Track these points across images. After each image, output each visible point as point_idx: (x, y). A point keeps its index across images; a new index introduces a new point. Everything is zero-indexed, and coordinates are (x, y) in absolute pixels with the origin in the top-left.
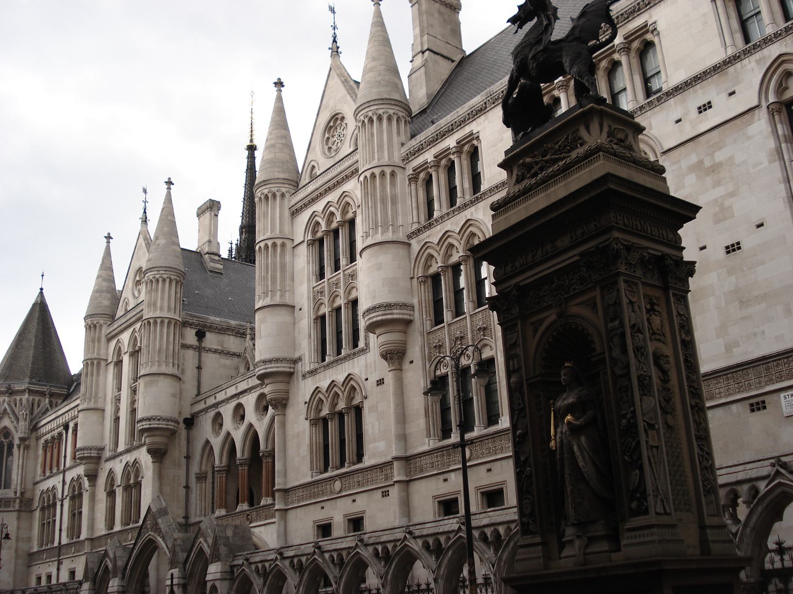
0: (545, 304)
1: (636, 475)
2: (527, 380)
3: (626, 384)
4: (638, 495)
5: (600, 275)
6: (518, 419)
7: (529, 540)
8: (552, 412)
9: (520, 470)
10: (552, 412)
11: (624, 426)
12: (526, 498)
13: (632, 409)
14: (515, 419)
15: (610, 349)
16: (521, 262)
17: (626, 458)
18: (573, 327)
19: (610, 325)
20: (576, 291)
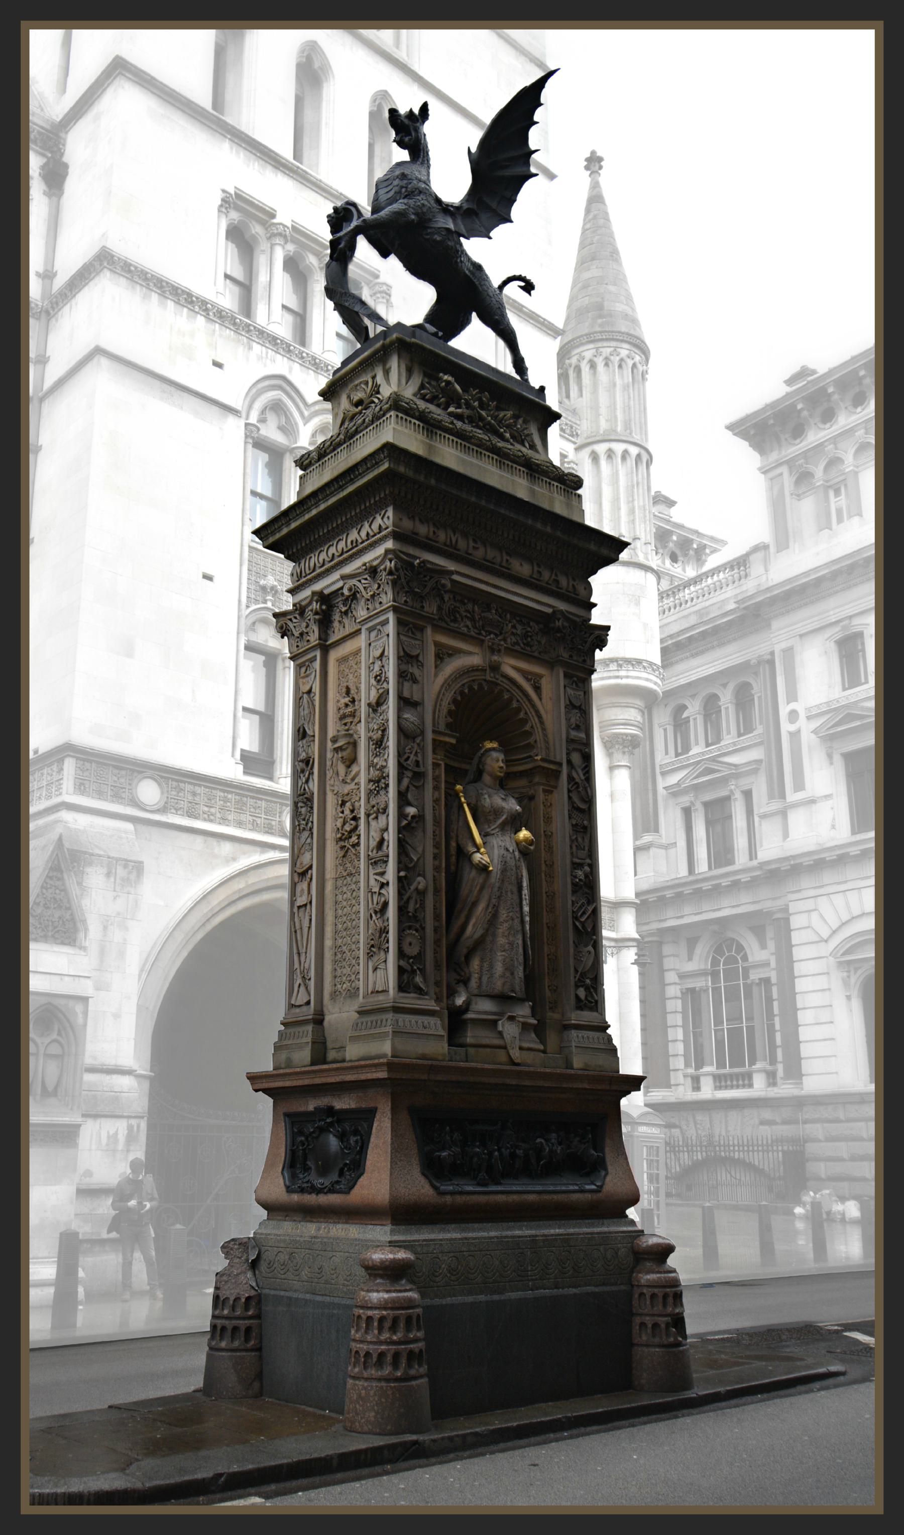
0: (465, 629)
1: (589, 952)
2: (434, 732)
3: (585, 822)
4: (588, 981)
5: (571, 656)
6: (408, 787)
7: (410, 1000)
8: (465, 806)
9: (405, 877)
10: (465, 806)
11: (580, 880)
12: (410, 928)
13: (588, 861)
14: (406, 781)
15: (569, 762)
16: (454, 541)
17: (577, 924)
18: (476, 687)
19: (573, 734)
20: (517, 648)
